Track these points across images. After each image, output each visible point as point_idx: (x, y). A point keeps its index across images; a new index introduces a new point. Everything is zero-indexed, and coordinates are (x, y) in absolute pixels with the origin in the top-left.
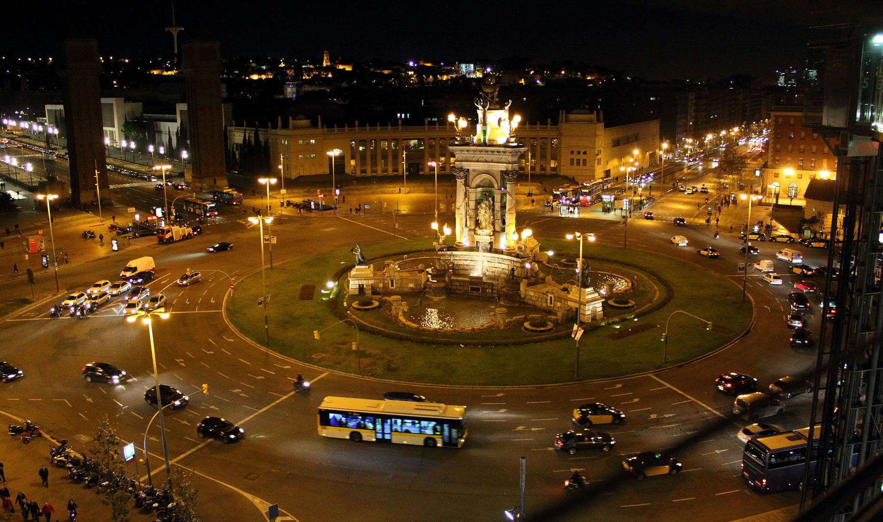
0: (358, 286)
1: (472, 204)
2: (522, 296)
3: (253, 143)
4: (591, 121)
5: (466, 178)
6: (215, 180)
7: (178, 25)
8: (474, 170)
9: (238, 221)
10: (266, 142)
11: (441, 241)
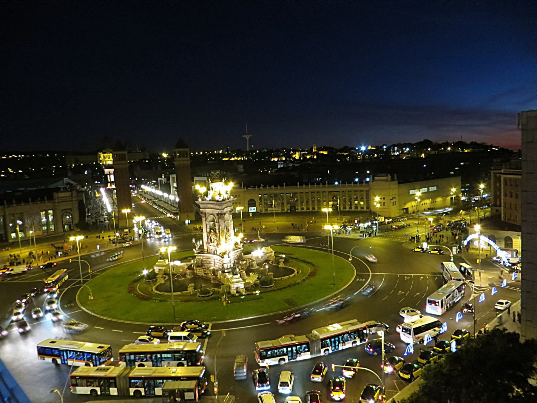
1: (208, 230)
2: (219, 278)
4: (387, 180)
5: (206, 216)
7: (249, 134)
8: (208, 213)
11: (197, 248)
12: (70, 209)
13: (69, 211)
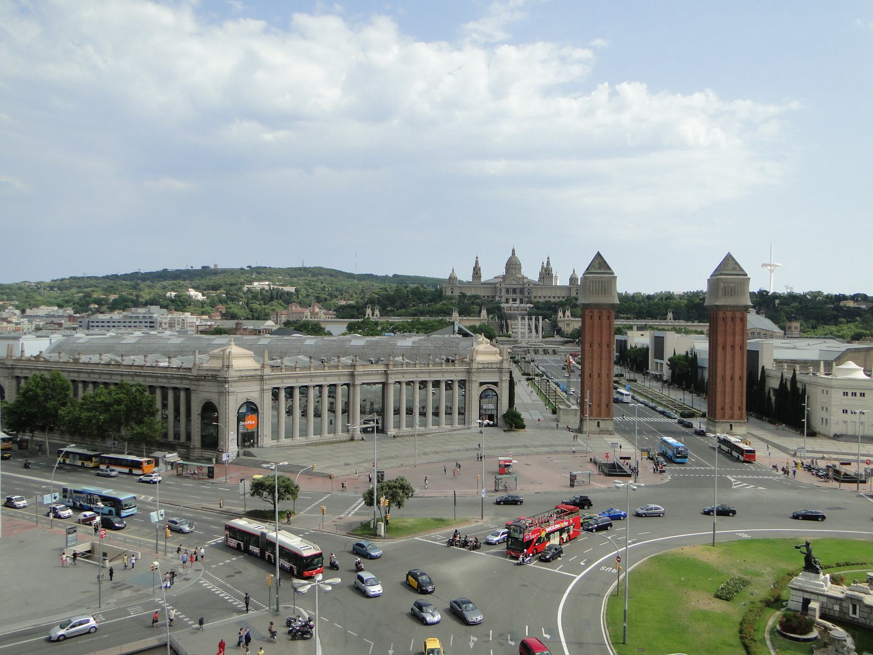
0: (801, 601)
3: (789, 389)
6: (731, 426)
9: (728, 476)
10: (804, 391)
12: (496, 384)
13: (492, 387)
